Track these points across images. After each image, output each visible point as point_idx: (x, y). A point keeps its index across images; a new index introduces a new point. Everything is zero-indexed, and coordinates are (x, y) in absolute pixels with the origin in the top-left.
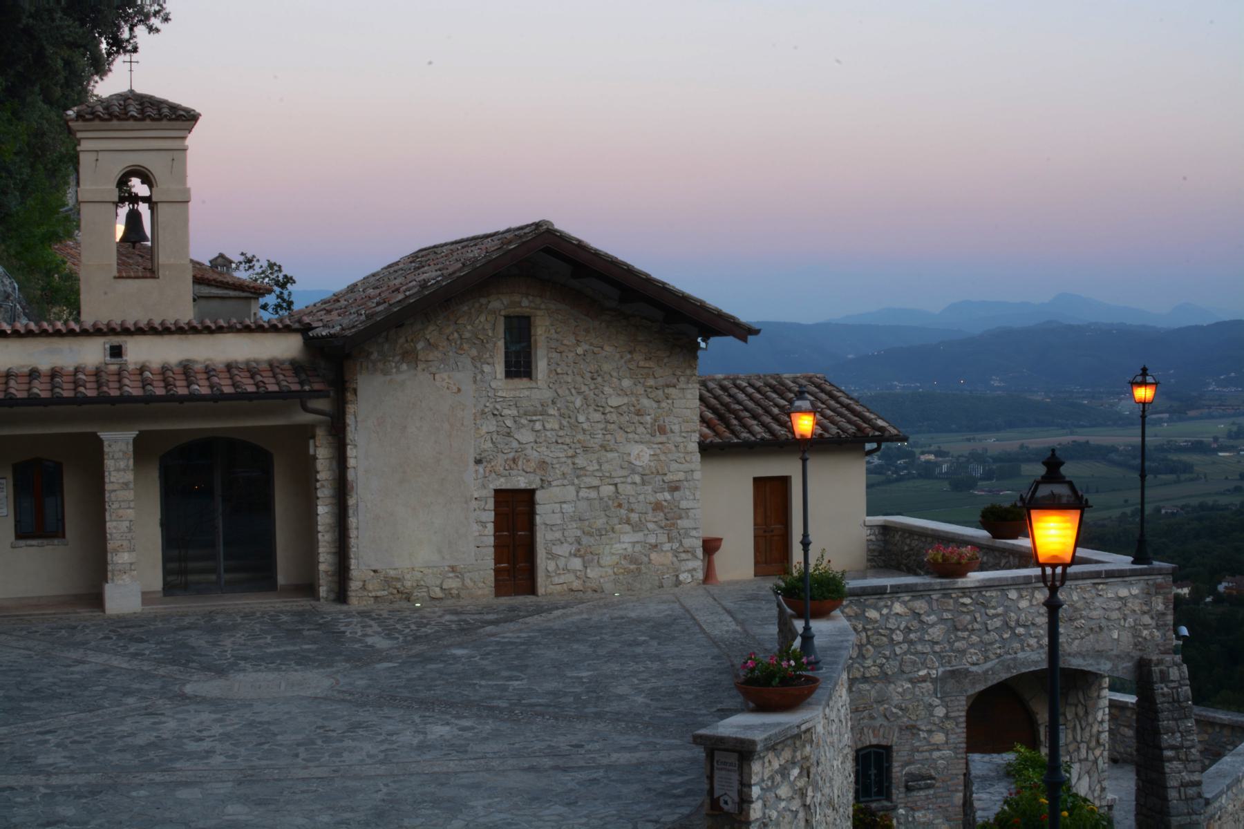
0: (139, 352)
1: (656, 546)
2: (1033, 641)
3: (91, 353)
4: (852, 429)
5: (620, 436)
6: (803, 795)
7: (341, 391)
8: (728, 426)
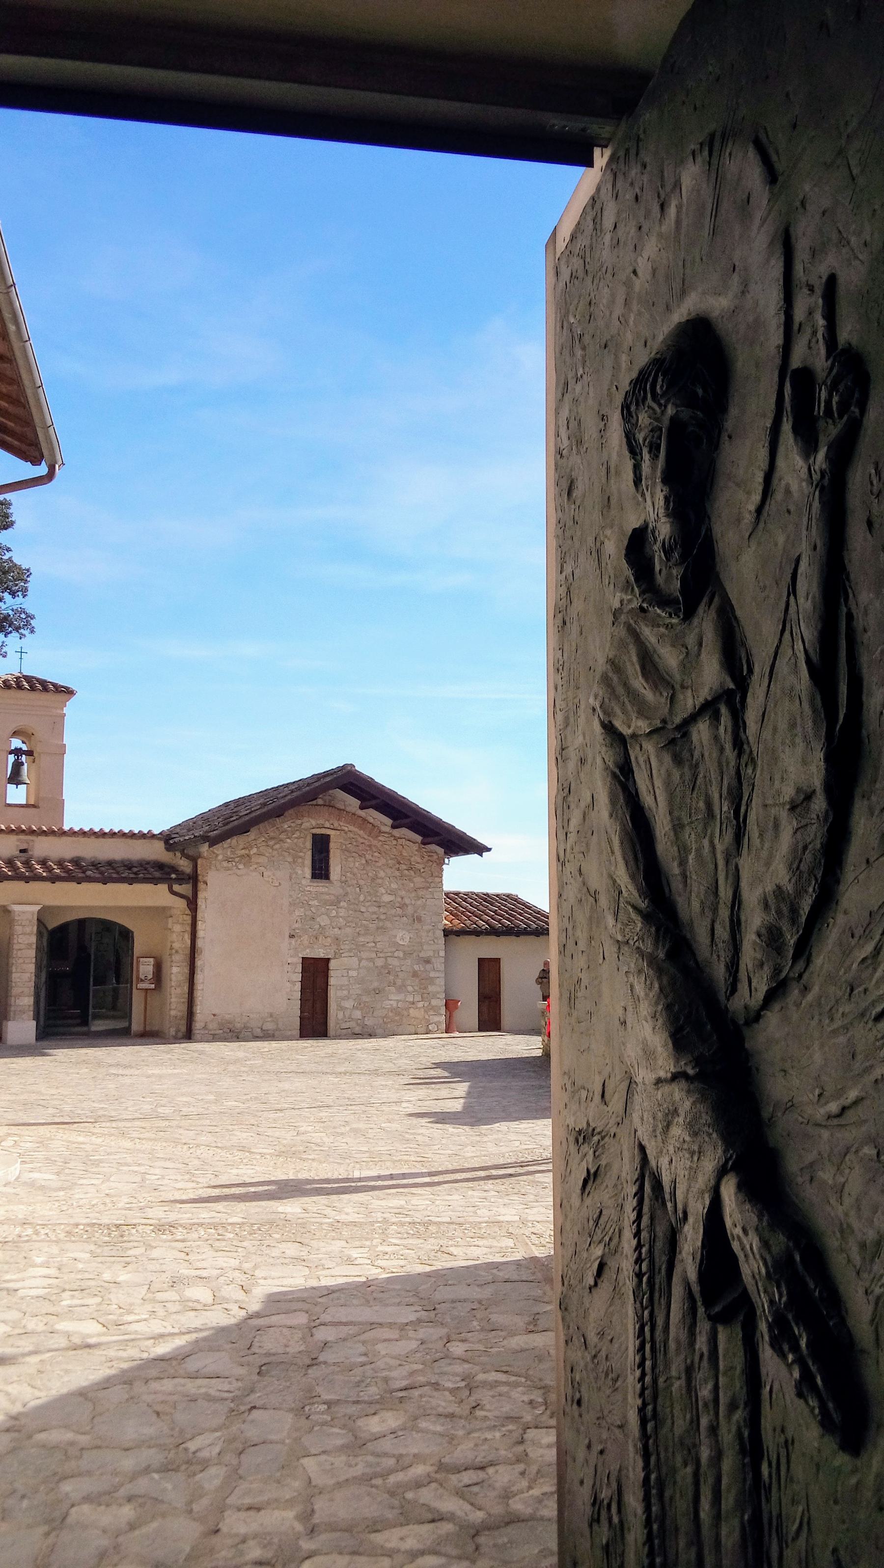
1: (413, 1003)
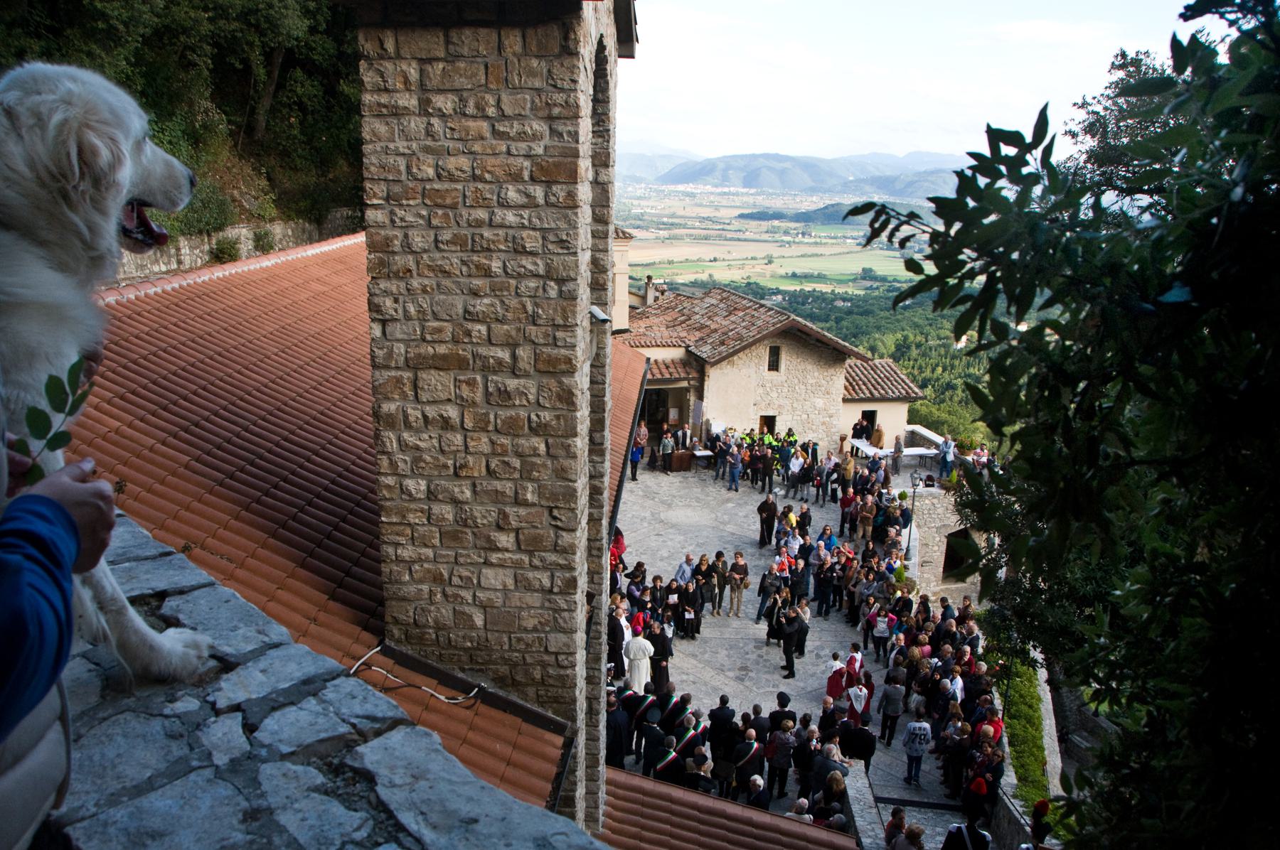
4: (903, 392)
8: (854, 389)
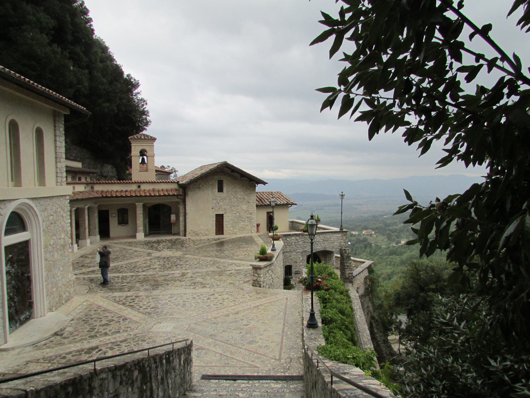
0: (143, 187)
2: (320, 245)
3: (134, 187)
5: (240, 203)
6: (272, 276)
7: (185, 194)
8: (262, 202)
